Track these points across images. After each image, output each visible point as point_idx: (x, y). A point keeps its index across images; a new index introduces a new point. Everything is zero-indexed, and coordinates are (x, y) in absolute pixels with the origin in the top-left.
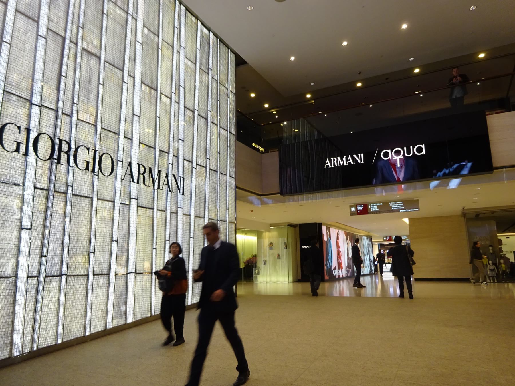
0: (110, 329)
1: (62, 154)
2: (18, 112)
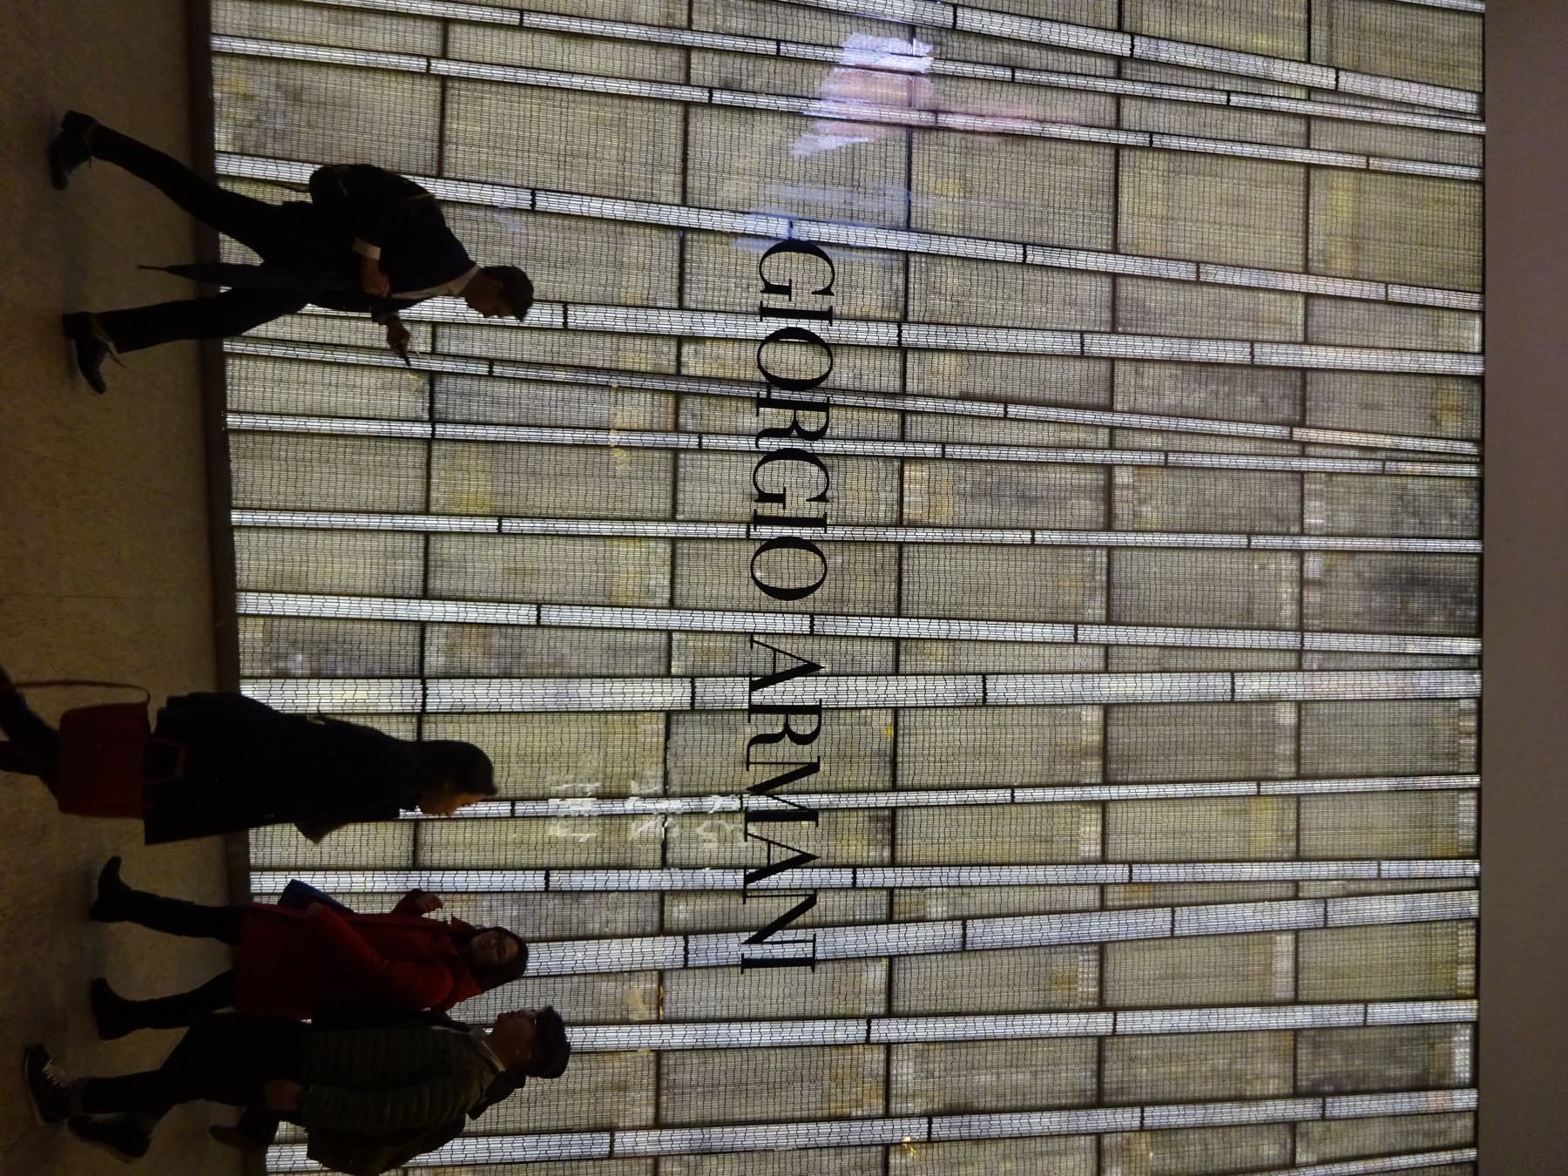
0: (232, 603)
1: (789, 413)
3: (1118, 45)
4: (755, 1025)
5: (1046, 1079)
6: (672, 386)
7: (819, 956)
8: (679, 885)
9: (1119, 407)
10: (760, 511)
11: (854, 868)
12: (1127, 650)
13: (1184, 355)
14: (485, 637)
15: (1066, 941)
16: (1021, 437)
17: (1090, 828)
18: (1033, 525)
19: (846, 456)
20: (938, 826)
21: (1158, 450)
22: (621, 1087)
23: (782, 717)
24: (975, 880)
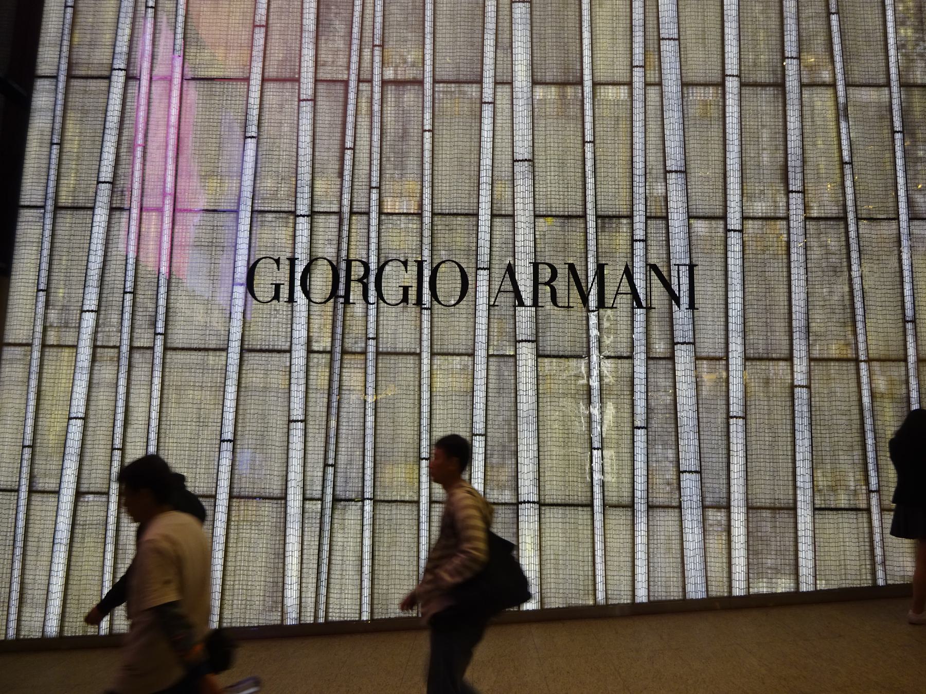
1: (353, 284)
2: (277, 236)
3: (119, 78)
4: (730, 301)
5: (767, 119)
6: (338, 356)
7: (688, 262)
8: (643, 348)
9: (345, 77)
10: (414, 302)
11: (633, 241)
12: (498, 70)
13: (313, 35)
14: (493, 467)
15: (680, 107)
16: (366, 140)
17: (610, 93)
18: (420, 131)
19: (379, 249)
20: (608, 188)
21: (373, 51)
22: (767, 382)
23: (540, 287)
24: (642, 165)
